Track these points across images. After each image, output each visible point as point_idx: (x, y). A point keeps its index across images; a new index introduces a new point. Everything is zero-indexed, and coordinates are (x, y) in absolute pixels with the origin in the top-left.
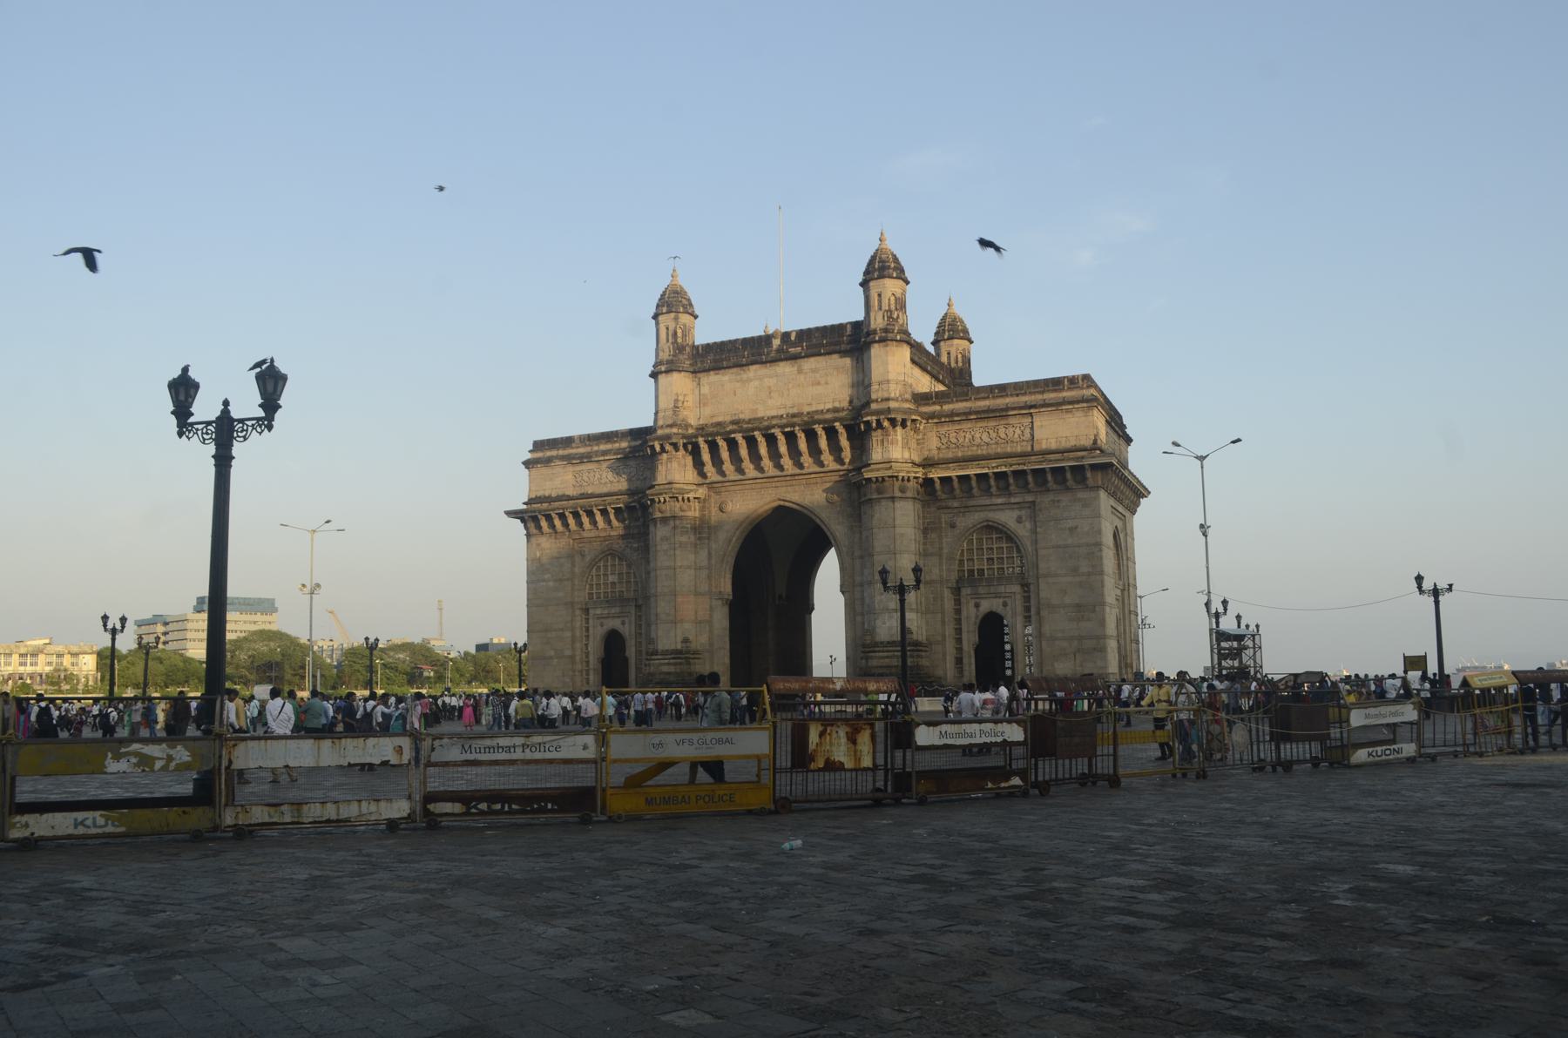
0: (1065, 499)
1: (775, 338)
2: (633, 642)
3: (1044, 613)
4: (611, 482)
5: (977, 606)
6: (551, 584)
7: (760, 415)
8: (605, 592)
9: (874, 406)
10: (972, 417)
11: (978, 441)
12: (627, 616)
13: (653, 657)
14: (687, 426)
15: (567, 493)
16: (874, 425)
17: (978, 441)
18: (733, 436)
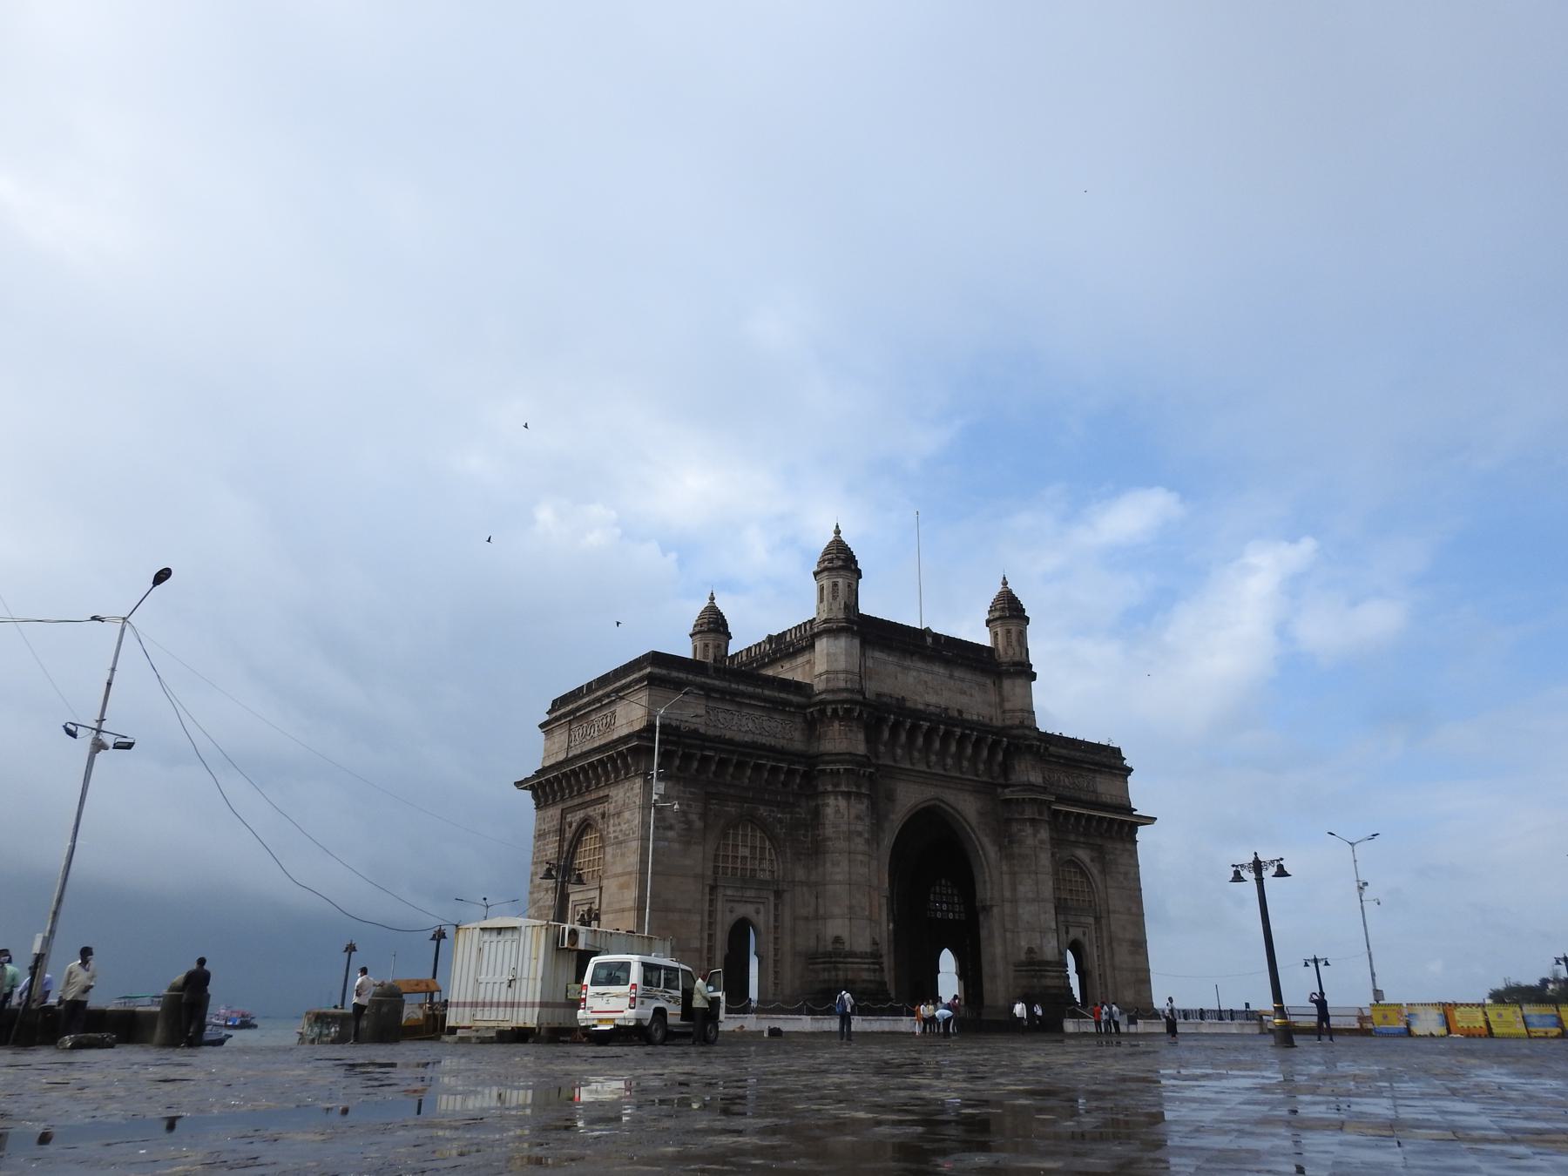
0: (1119, 846)
1: (929, 636)
2: (771, 938)
3: (1115, 945)
4: (753, 733)
5: (1067, 933)
6: (676, 846)
7: (921, 707)
8: (733, 868)
9: (1027, 732)
10: (1062, 761)
11: (1062, 783)
12: (763, 903)
13: (850, 960)
14: (864, 698)
15: (701, 731)
16: (1035, 749)
17: (1062, 783)
18: (921, 723)
